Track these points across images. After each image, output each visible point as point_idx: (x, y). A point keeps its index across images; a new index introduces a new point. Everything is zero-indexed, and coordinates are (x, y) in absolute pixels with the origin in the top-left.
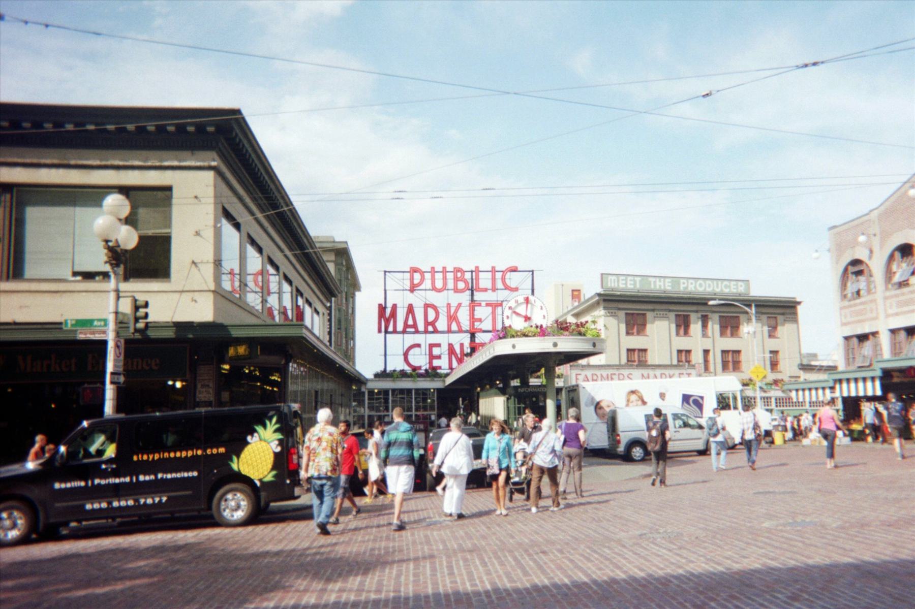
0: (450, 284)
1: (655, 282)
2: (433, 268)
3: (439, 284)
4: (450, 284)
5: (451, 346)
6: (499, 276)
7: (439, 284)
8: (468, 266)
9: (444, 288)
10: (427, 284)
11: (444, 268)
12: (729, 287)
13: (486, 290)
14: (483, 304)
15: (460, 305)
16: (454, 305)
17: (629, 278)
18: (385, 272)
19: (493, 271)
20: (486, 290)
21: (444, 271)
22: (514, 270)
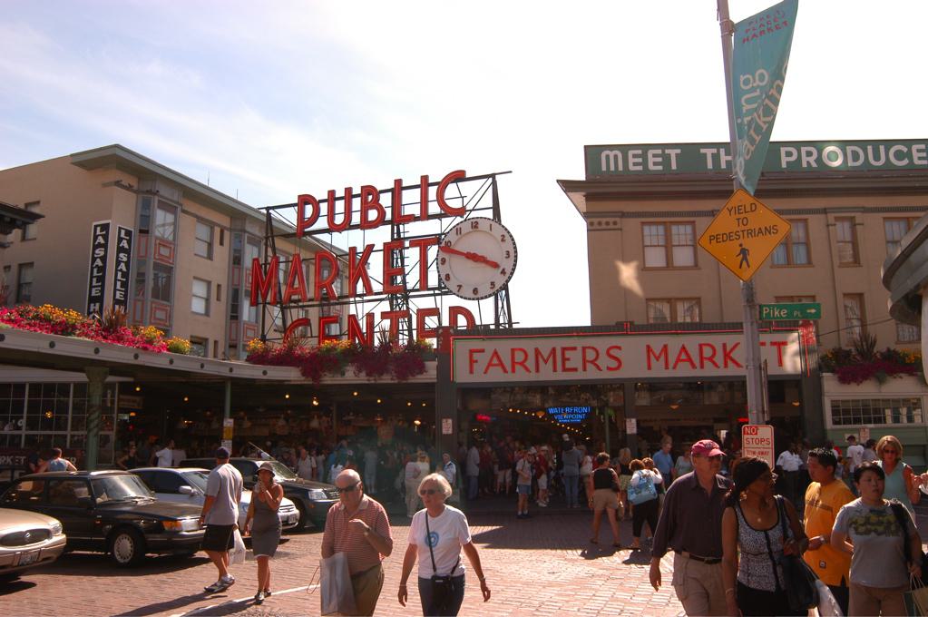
0: (356, 219)
1: (716, 157)
2: (332, 193)
3: (339, 220)
4: (356, 219)
5: (353, 318)
6: (433, 191)
7: (339, 220)
8: (384, 182)
9: (347, 226)
10: (322, 223)
11: (348, 190)
12: (909, 155)
13: (412, 218)
14: (407, 244)
15: (369, 249)
16: (360, 249)
17: (651, 153)
18: (268, 209)
19: (425, 183)
20: (412, 218)
21: (349, 195)
22: (458, 177)
